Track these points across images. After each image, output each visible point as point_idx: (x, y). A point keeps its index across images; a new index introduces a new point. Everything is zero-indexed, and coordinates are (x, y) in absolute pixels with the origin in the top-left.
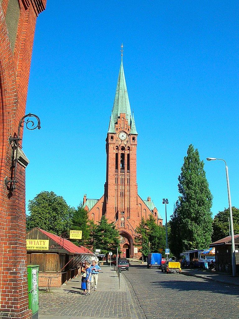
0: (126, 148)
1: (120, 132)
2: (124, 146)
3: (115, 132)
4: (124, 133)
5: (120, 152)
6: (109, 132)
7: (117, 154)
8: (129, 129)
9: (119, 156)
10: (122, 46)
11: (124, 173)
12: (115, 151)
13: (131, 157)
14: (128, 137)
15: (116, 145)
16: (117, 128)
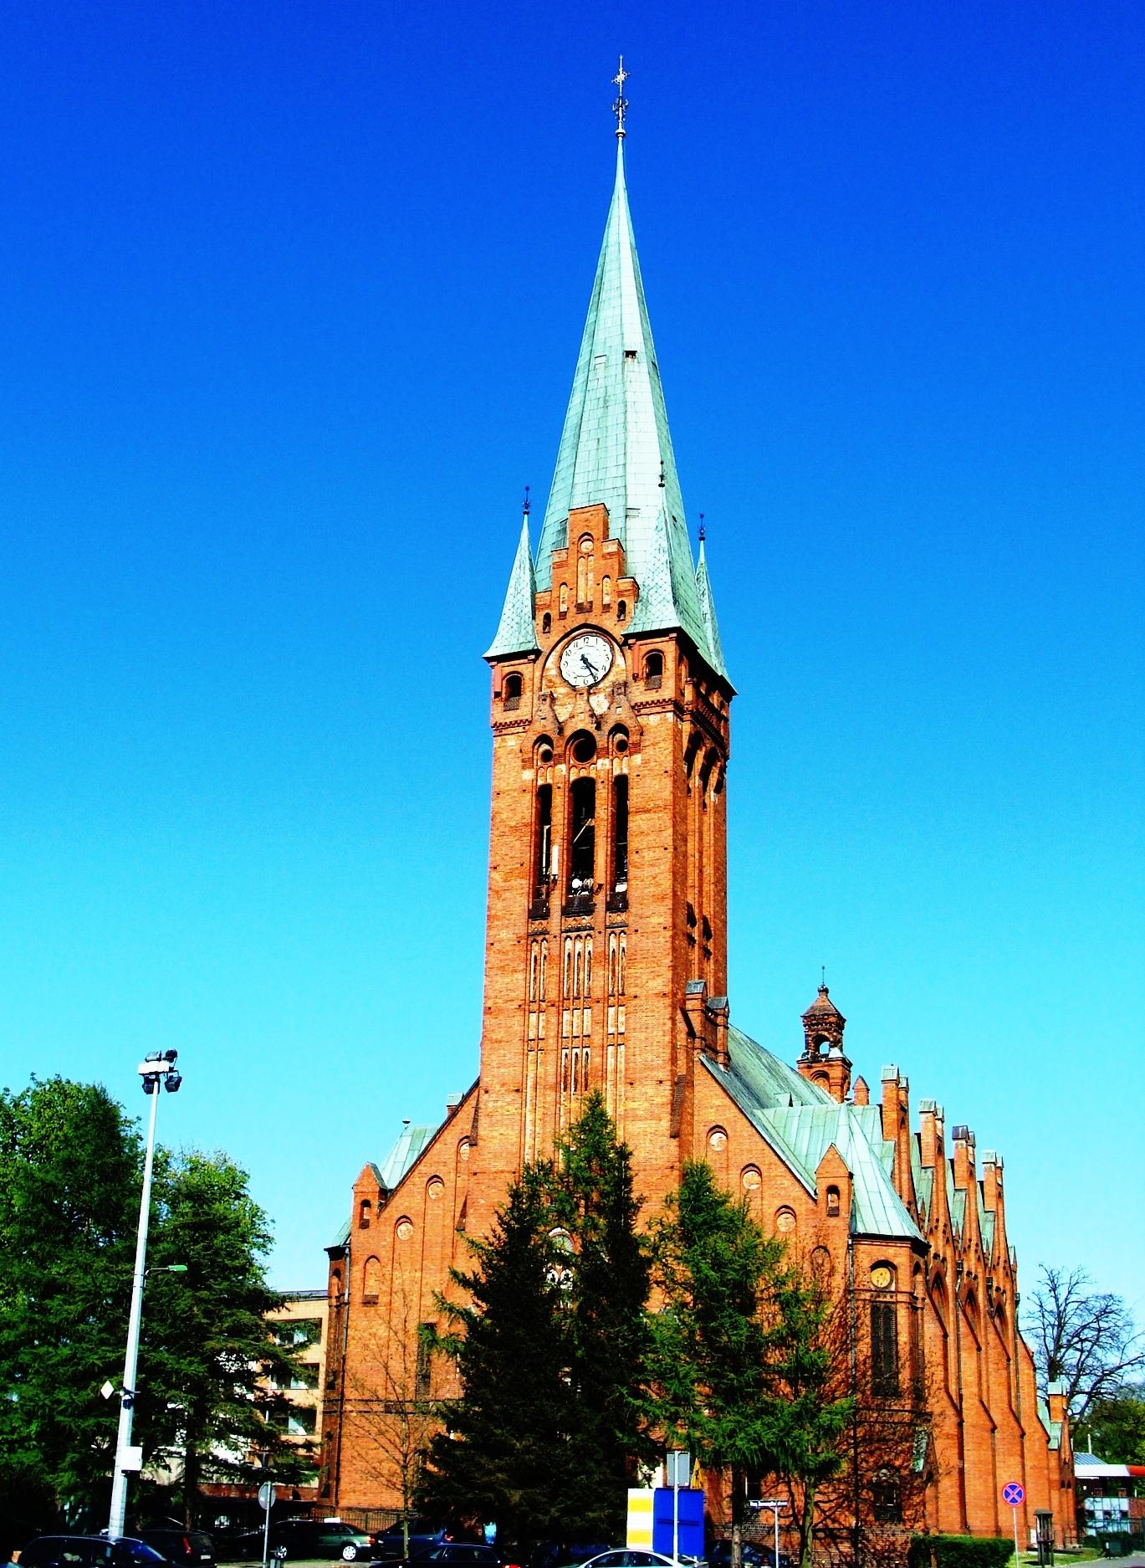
0: (601, 739)
1: (568, 636)
2: (591, 728)
3: (530, 647)
4: (592, 640)
5: (563, 773)
6: (489, 654)
7: (544, 795)
8: (622, 605)
9: (560, 802)
10: (621, 78)
11: (586, 920)
12: (528, 775)
13: (635, 797)
14: (619, 660)
15: (538, 727)
16: (547, 617)
